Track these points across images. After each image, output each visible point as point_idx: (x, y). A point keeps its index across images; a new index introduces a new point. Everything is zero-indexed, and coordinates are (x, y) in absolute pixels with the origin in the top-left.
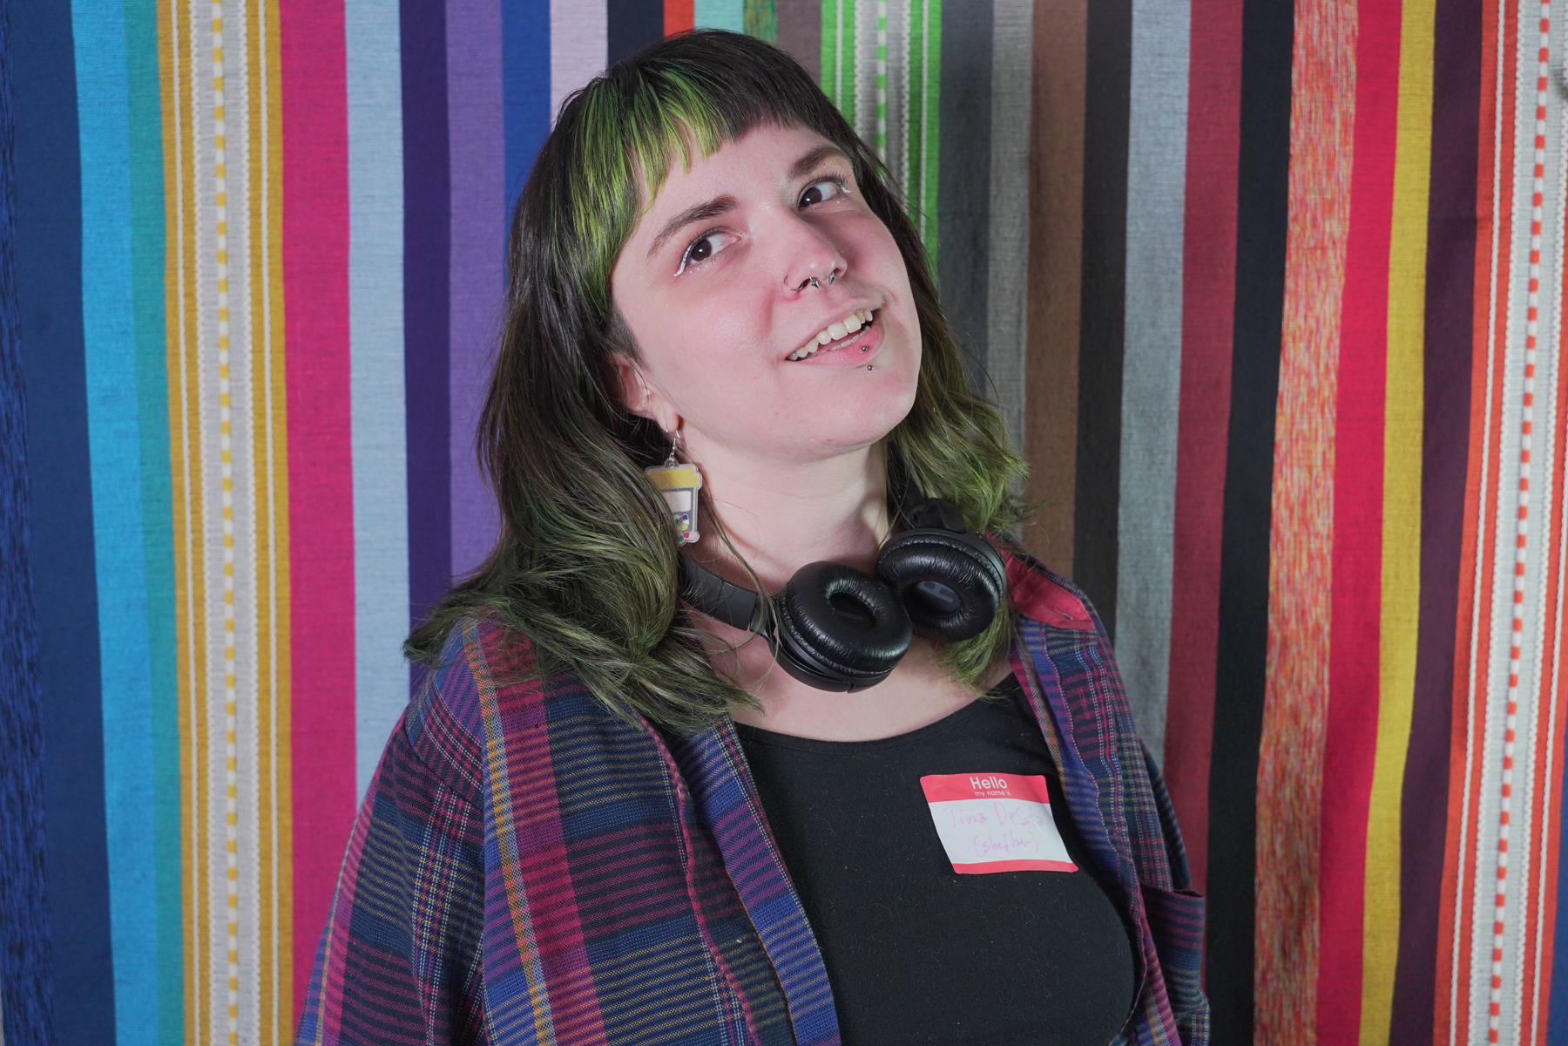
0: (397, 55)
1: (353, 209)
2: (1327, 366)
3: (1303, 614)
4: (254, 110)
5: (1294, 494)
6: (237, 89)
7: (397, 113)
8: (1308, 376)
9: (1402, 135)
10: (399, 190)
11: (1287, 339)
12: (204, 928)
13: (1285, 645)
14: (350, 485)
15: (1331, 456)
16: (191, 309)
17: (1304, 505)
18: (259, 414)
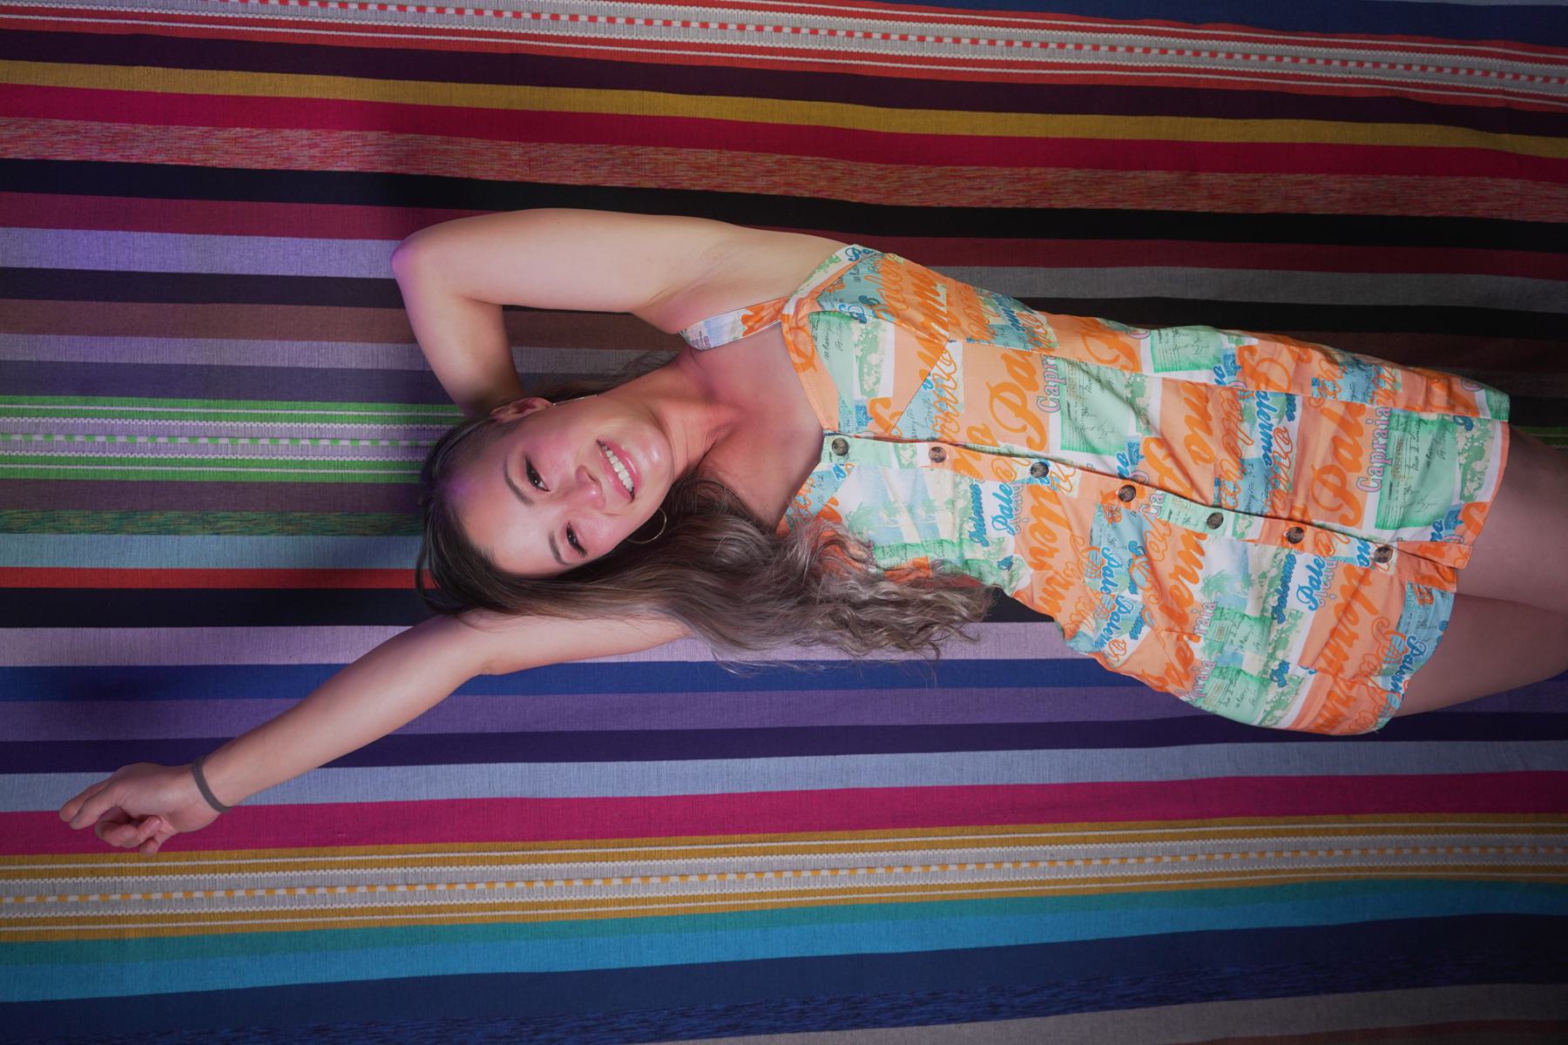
0: (392, 769)
1: (498, 795)
2: (611, 152)
3: (770, 172)
4: (431, 863)
5: (692, 174)
6: (416, 874)
7: (432, 767)
8: (614, 166)
9: (455, 103)
10: (484, 766)
11: (590, 182)
12: (979, 885)
13: (790, 184)
14: (684, 797)
15: (667, 149)
16: (565, 904)
17: (699, 168)
18: (636, 857)
